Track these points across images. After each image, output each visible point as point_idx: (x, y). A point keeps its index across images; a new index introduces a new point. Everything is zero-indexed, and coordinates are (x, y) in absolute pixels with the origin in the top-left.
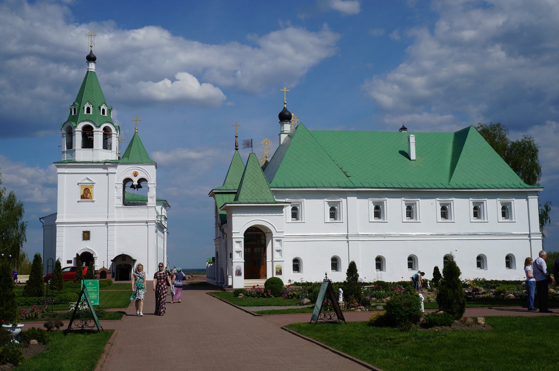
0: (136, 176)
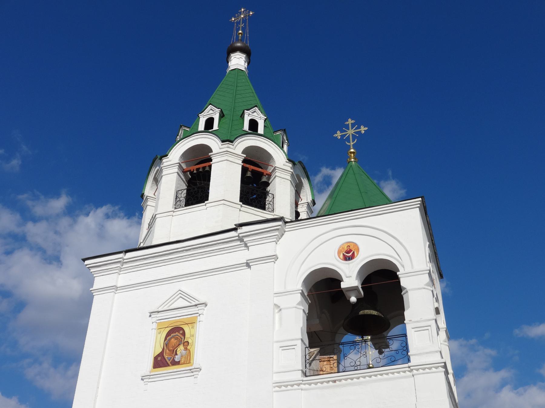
0: (352, 258)
